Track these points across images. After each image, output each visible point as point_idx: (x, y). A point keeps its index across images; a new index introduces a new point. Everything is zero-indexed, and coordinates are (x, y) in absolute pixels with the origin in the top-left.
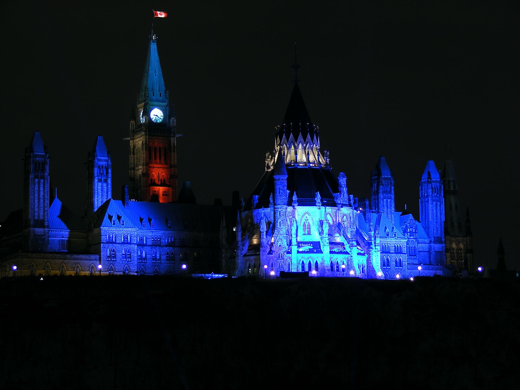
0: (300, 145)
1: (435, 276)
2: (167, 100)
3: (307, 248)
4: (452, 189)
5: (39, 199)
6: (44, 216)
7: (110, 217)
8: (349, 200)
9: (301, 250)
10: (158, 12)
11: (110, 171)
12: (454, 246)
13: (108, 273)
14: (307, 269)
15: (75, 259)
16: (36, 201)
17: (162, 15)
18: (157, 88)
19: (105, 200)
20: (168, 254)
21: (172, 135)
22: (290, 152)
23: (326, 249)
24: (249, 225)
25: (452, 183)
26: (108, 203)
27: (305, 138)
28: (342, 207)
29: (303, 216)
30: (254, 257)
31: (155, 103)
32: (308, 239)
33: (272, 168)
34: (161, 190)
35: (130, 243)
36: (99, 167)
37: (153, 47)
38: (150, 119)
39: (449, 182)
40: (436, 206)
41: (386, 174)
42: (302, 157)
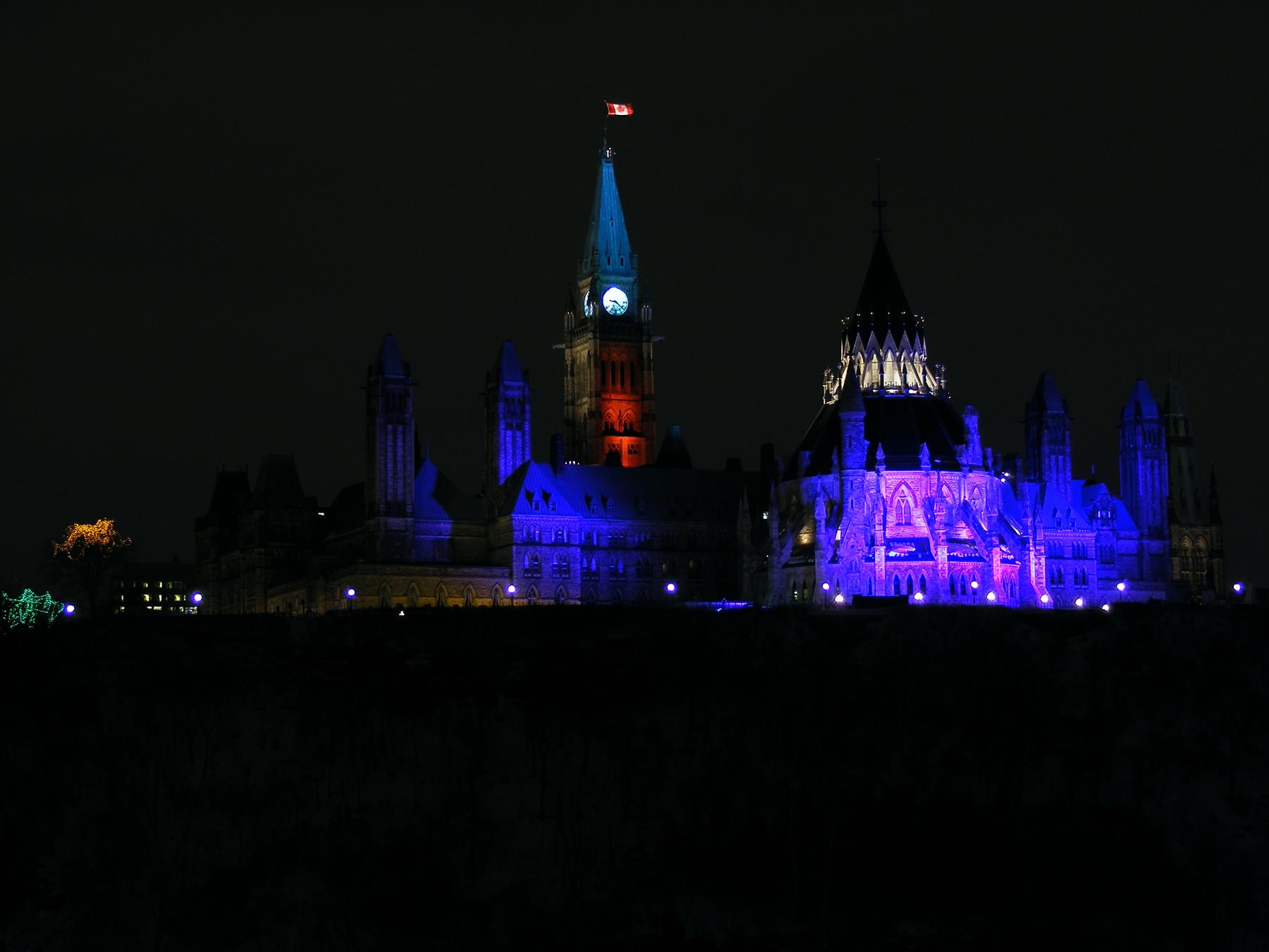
0: (889, 354)
1: (1151, 601)
2: (634, 272)
4: (1182, 434)
5: (395, 462)
7: (530, 496)
8: (985, 457)
9: (892, 554)
10: (616, 106)
11: (528, 407)
12: (1187, 543)
13: (525, 601)
14: (904, 591)
15: (464, 575)
16: (390, 466)
17: (621, 111)
18: (614, 249)
19: (519, 463)
20: (639, 563)
21: (645, 338)
22: (870, 369)
23: (942, 554)
24: (793, 508)
26: (525, 466)
27: (898, 340)
29: (896, 489)
30: (803, 568)
31: (613, 278)
32: (906, 532)
33: (836, 397)
34: (625, 442)
35: (568, 545)
37: (608, 171)
38: (603, 309)
40: (1153, 469)
42: (892, 378)
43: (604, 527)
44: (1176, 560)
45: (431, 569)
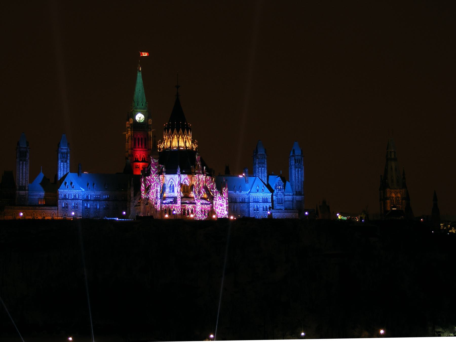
3: (169, 200)
4: (393, 157)
5: (23, 173)
6: (25, 184)
7: (66, 183)
9: (164, 202)
11: (69, 155)
12: (393, 195)
15: (42, 209)
16: (21, 175)
17: (145, 54)
19: (65, 173)
23: (179, 202)
25: (393, 154)
27: (183, 132)
28: (195, 174)
31: (139, 110)
32: (172, 194)
34: (141, 164)
35: (78, 199)
36: (62, 153)
37: (139, 75)
39: (391, 152)
41: (261, 151)
43: (92, 194)
44: (388, 201)
45: (30, 208)
